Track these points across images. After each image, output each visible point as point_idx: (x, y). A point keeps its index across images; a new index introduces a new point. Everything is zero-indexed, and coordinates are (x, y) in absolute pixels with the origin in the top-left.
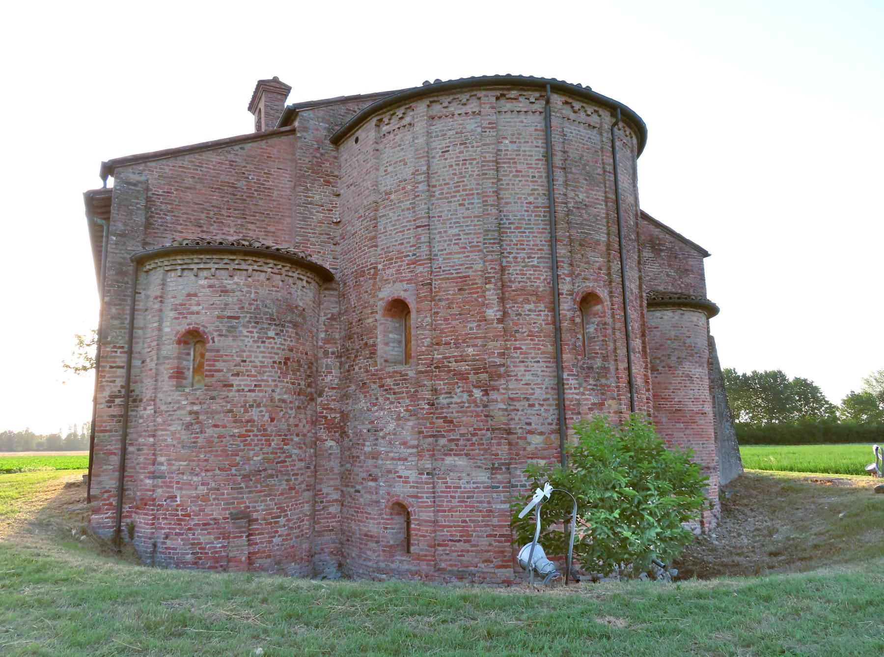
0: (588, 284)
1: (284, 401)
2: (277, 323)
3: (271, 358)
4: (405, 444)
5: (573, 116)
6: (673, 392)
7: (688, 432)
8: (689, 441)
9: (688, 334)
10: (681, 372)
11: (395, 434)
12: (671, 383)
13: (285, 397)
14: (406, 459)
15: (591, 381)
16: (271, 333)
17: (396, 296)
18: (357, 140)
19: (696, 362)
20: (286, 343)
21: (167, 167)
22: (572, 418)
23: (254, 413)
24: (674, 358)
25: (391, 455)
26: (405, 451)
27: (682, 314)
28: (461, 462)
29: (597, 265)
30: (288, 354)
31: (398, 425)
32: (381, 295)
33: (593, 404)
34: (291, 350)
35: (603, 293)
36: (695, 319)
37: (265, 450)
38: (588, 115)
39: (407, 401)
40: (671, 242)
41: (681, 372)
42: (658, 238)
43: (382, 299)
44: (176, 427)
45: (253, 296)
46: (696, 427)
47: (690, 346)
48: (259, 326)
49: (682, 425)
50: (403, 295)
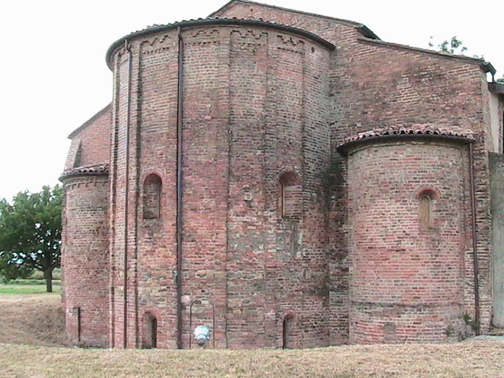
0: (151, 168)
1: (96, 250)
2: (92, 209)
3: (88, 228)
5: (151, 48)
6: (367, 230)
7: (378, 269)
8: (379, 278)
9: (382, 170)
10: (373, 210)
12: (366, 222)
13: (97, 248)
15: (147, 236)
16: (89, 216)
19: (391, 198)
20: (98, 219)
21: (88, 131)
22: (131, 261)
23: (81, 258)
24: (368, 197)
27: (375, 151)
29: (160, 152)
30: (99, 225)
33: (146, 251)
34: (101, 223)
35: (161, 172)
36: (392, 153)
37: (86, 276)
38: (162, 42)
40: (435, 64)
41: (373, 210)
42: (419, 65)
45: (81, 197)
46: (387, 264)
47: (382, 183)
48: (83, 212)
49: (373, 262)
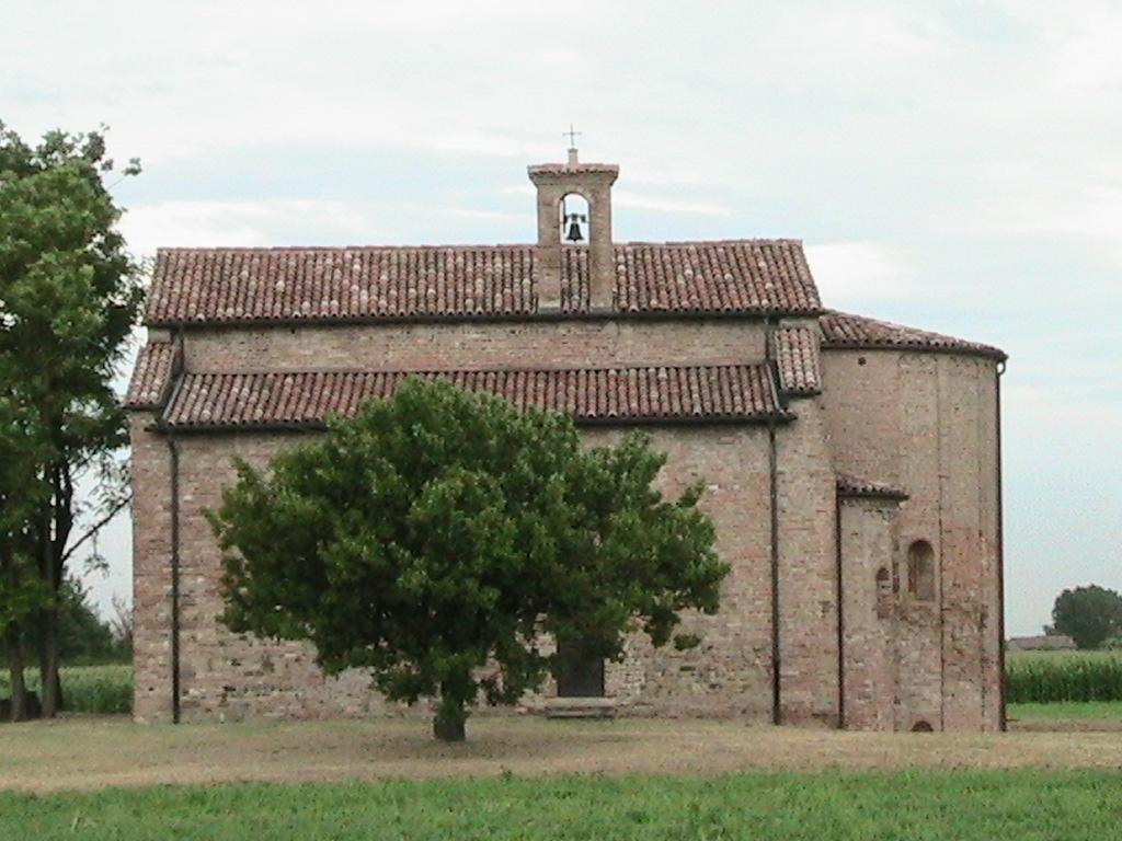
4: (929, 671)
11: (919, 662)
14: (930, 685)
17: (920, 537)
18: (862, 362)
25: (916, 680)
26: (930, 677)
28: (968, 686)
31: (921, 655)
32: (904, 533)
39: (932, 633)
43: (906, 537)
44: (879, 654)
50: (927, 537)
